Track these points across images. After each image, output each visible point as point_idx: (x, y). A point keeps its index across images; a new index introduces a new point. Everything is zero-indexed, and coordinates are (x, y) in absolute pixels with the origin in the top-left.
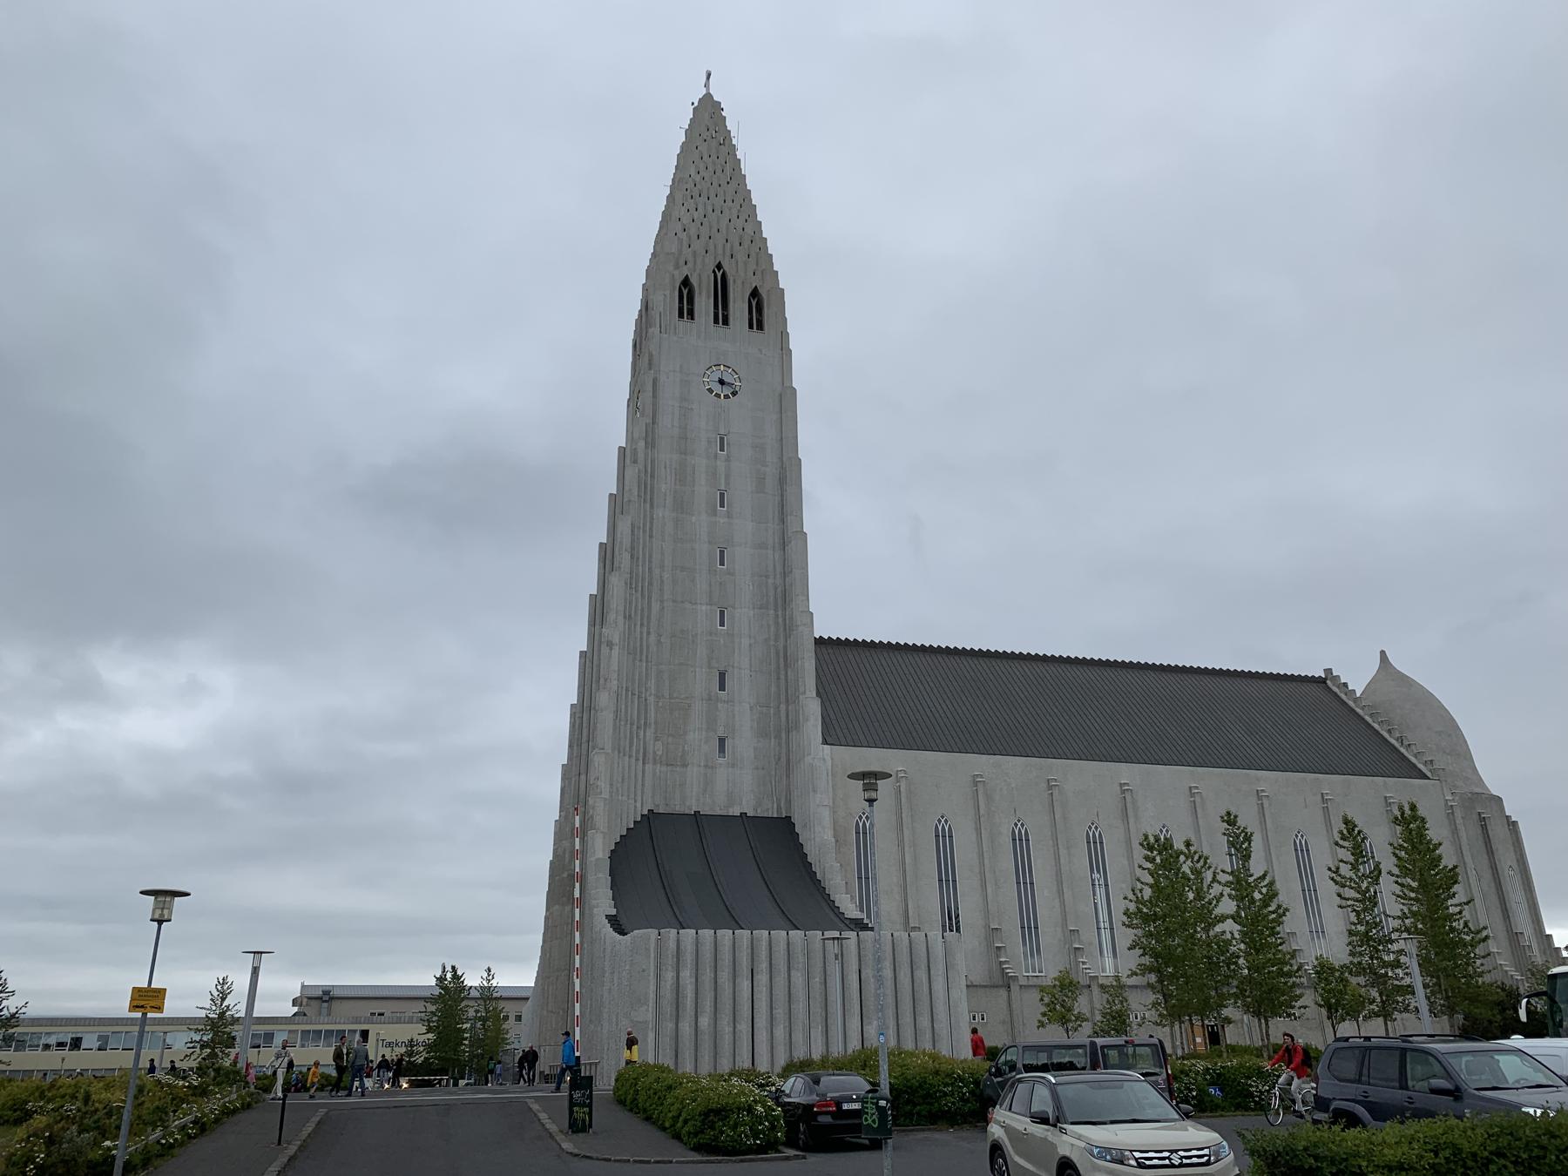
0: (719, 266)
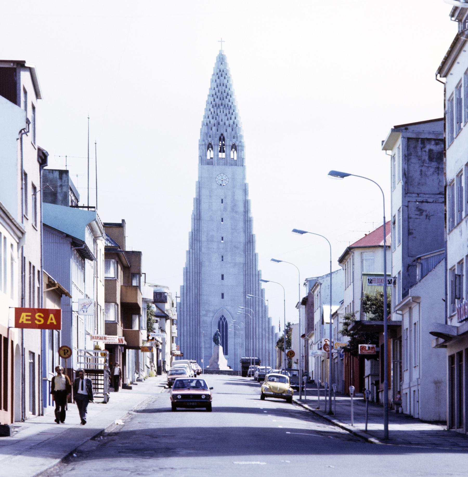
0: (222, 135)
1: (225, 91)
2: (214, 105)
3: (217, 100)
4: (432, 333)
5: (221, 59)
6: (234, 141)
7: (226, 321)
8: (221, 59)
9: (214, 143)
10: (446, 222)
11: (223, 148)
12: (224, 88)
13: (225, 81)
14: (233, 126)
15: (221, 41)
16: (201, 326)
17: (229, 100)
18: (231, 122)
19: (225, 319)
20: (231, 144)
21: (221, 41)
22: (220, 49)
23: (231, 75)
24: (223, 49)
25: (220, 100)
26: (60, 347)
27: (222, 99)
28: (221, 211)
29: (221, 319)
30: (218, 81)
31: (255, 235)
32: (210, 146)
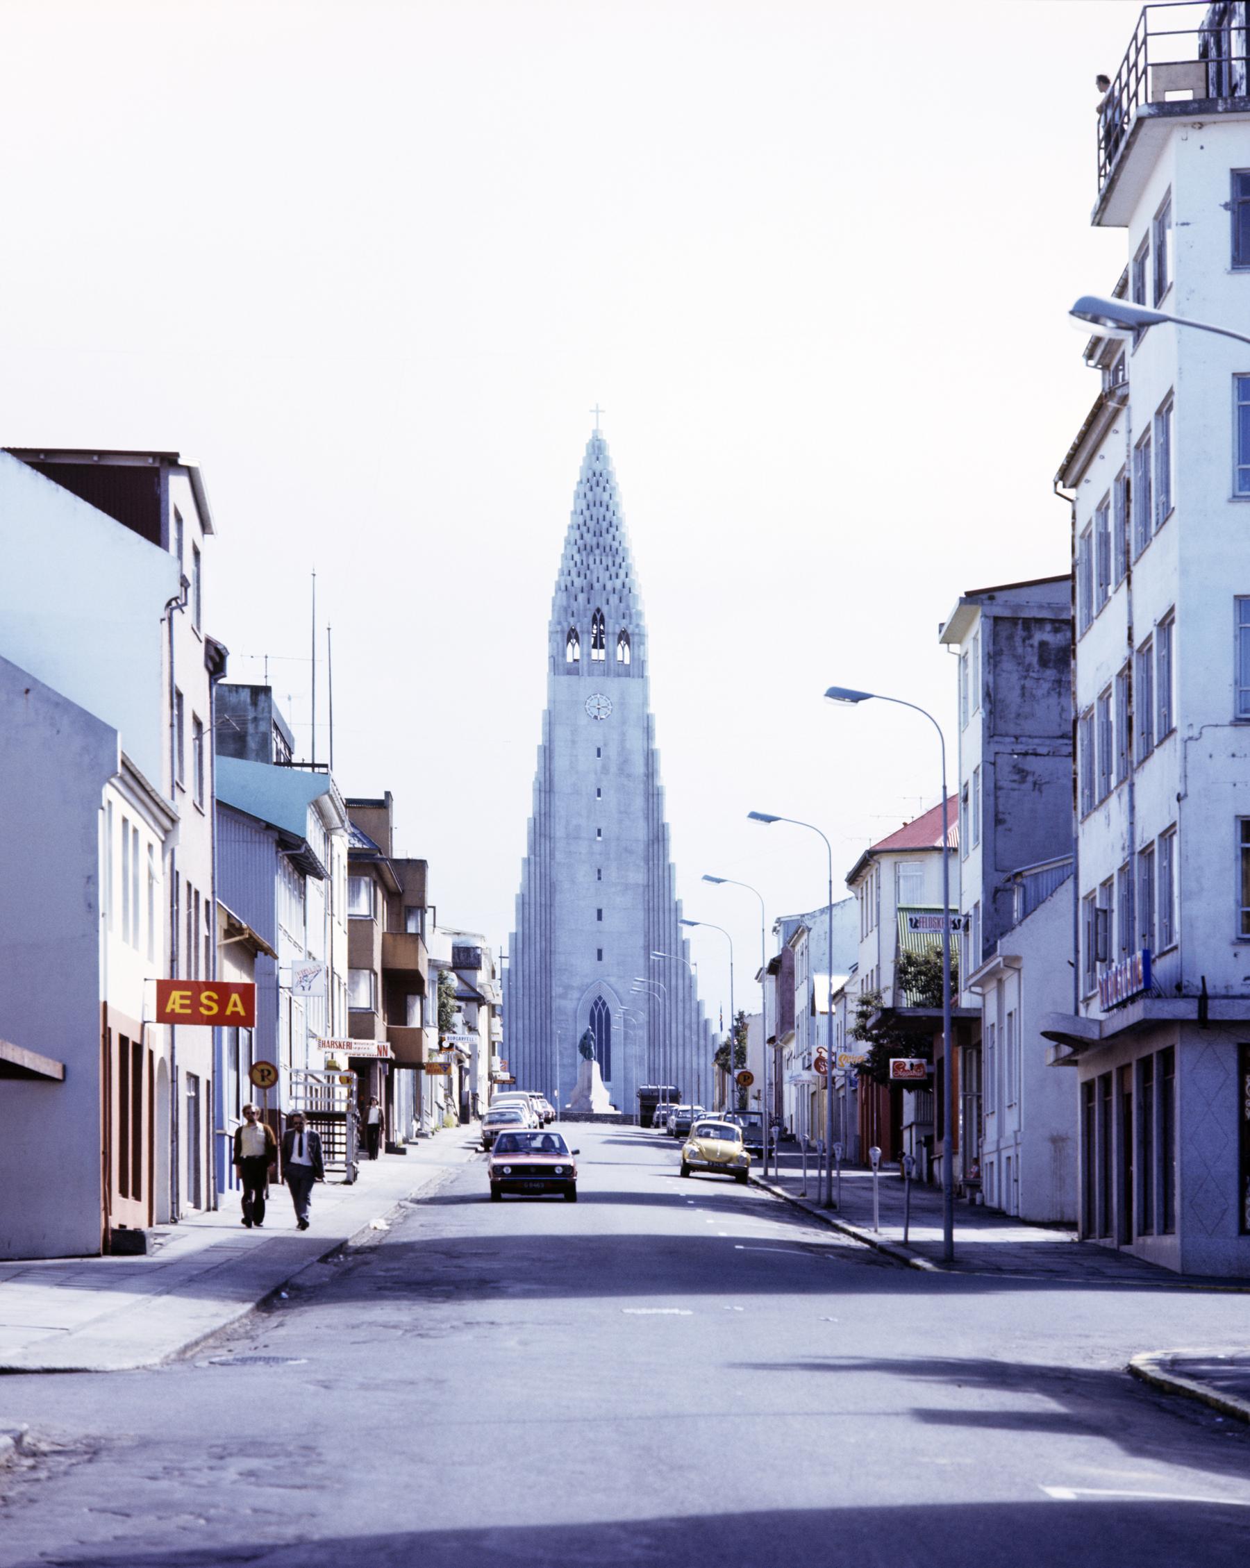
0: (598, 610)
1: (604, 516)
2: (582, 548)
3: (588, 537)
4: (1047, 1035)
5: (597, 450)
6: (624, 623)
7: (608, 1008)
8: (597, 450)
9: (581, 627)
10: (1075, 797)
11: (601, 639)
12: (603, 510)
13: (606, 497)
14: (621, 591)
15: (597, 411)
16: (554, 1018)
17: (614, 537)
18: (618, 583)
19: (604, 1004)
20: (618, 631)
21: (597, 411)
22: (595, 428)
23: (617, 484)
24: (600, 428)
25: (595, 535)
26: (253, 1063)
27: (598, 533)
28: (596, 774)
29: (596, 1004)
30: (590, 495)
31: (668, 824)
32: (573, 635)
